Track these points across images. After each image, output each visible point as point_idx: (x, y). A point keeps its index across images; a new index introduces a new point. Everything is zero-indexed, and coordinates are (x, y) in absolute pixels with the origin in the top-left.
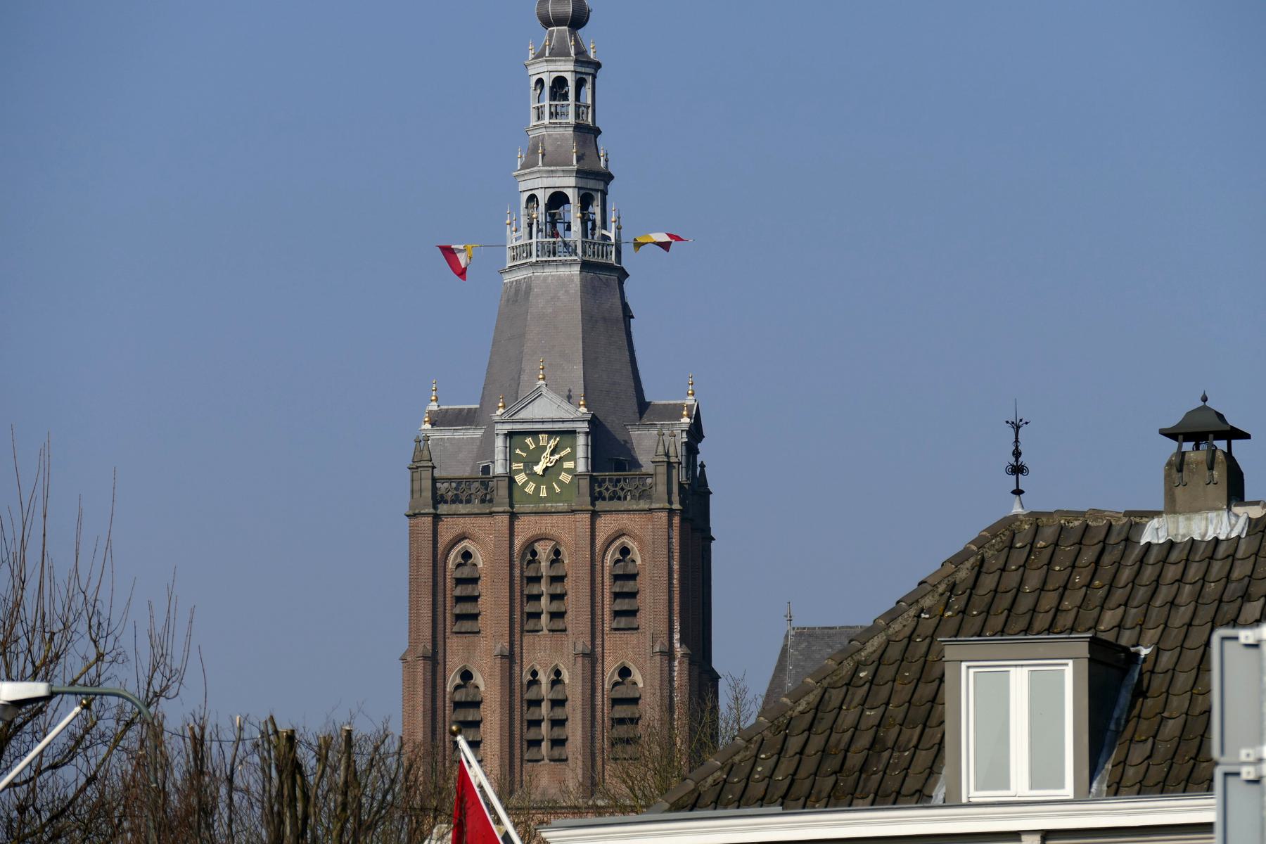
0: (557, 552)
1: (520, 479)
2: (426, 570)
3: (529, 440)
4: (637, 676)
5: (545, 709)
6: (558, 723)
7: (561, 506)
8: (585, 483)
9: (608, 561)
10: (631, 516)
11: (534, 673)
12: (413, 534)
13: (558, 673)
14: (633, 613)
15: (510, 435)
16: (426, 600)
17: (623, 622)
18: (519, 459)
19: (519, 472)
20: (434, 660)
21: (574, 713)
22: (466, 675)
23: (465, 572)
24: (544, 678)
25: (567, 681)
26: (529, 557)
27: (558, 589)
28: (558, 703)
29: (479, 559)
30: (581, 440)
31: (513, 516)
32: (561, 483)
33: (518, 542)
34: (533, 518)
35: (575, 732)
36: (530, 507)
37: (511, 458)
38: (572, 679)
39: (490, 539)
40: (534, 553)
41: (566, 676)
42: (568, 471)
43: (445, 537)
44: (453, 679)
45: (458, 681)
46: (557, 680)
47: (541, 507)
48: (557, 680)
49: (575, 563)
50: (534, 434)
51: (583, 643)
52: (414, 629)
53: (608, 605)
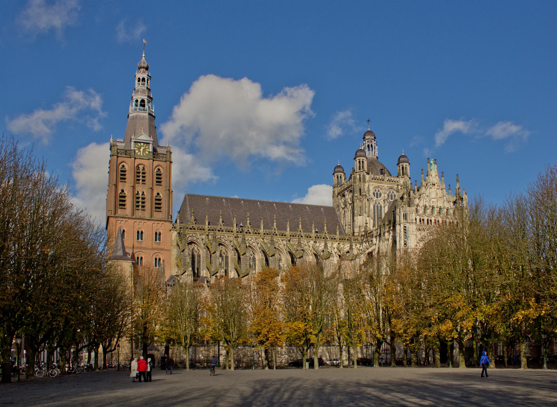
0: (144, 168)
1: (137, 151)
3: (139, 144)
4: (161, 195)
5: (140, 199)
6: (143, 203)
7: (146, 158)
8: (152, 154)
9: (156, 171)
10: (161, 162)
11: (138, 192)
13: (143, 192)
14: (160, 182)
15: (135, 142)
17: (158, 184)
18: (137, 147)
19: (136, 150)
22: (123, 191)
23: (123, 169)
24: (140, 193)
25: (145, 194)
26: (137, 168)
27: (144, 175)
28: (143, 199)
29: (127, 167)
30: (151, 145)
31: (135, 158)
32: (146, 154)
33: (136, 164)
34: (139, 160)
35: (148, 205)
36: (139, 157)
37: (135, 147)
38: (147, 194)
39: (129, 163)
40: (139, 168)
41: (145, 193)
42: (147, 151)
43: (119, 162)
44: (120, 191)
45: (121, 192)
47: (141, 158)
53: (155, 180)
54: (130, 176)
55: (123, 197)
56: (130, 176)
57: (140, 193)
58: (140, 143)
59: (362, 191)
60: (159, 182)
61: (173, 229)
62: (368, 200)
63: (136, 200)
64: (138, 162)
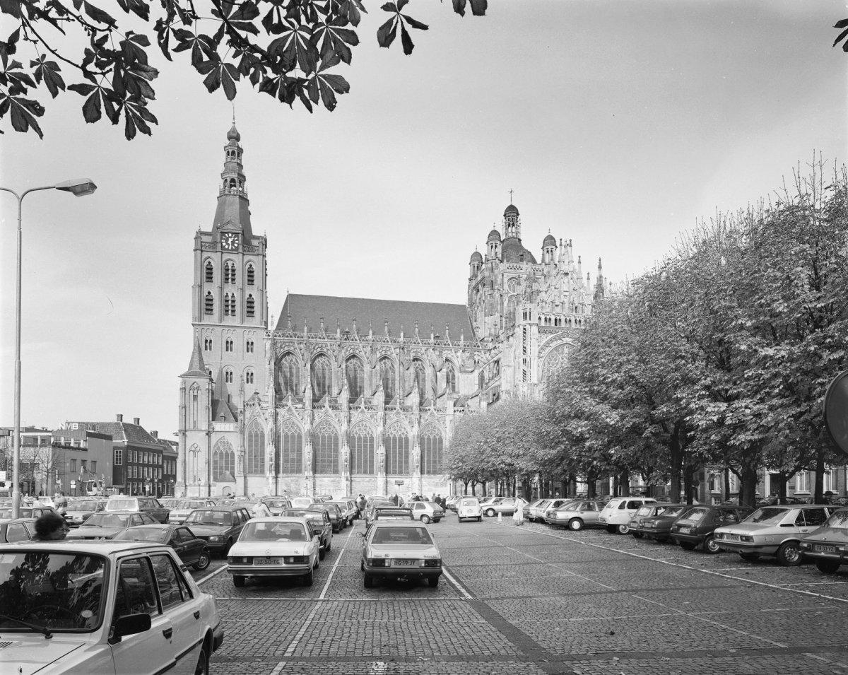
2: (199, 265)
12: (195, 256)
16: (199, 272)
20: (201, 286)
21: (238, 304)
24: (230, 295)
30: (240, 235)
35: (238, 308)
46: (233, 296)
48: (233, 296)
49: (238, 267)
50: (228, 233)
51: (241, 286)
52: (195, 279)
54: (217, 275)
55: (209, 301)
56: (217, 275)
57: (230, 295)
58: (228, 233)
59: (494, 284)
60: (251, 281)
61: (267, 337)
62: (501, 295)
63: (224, 303)
64: (226, 256)
